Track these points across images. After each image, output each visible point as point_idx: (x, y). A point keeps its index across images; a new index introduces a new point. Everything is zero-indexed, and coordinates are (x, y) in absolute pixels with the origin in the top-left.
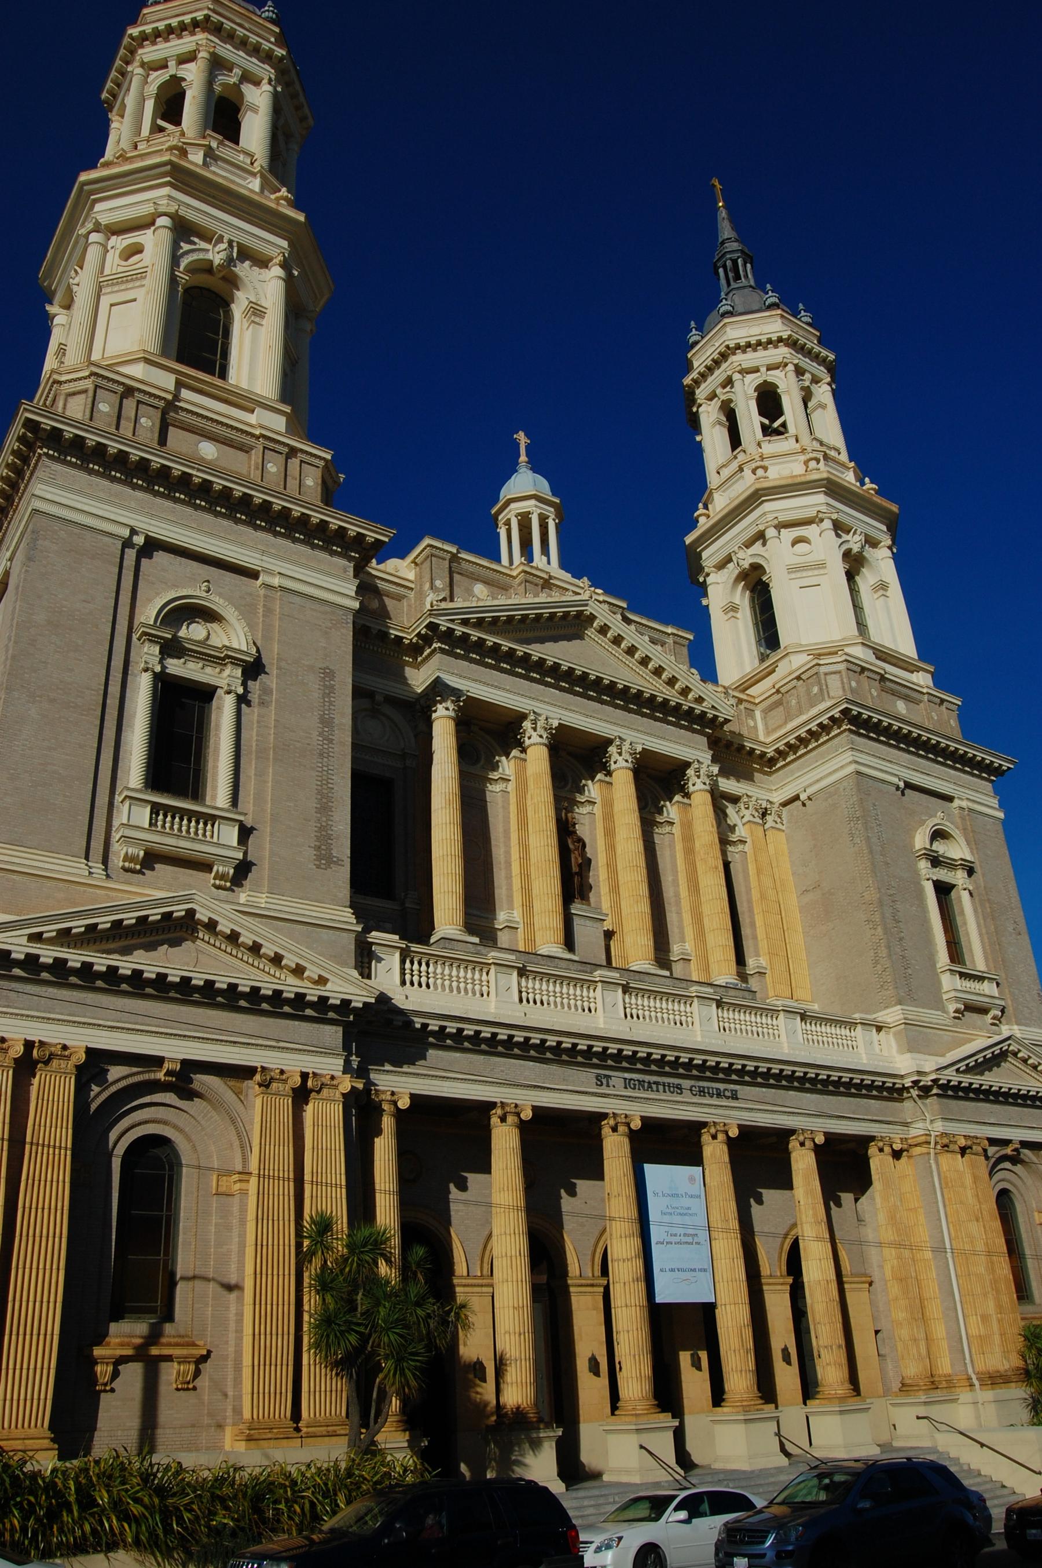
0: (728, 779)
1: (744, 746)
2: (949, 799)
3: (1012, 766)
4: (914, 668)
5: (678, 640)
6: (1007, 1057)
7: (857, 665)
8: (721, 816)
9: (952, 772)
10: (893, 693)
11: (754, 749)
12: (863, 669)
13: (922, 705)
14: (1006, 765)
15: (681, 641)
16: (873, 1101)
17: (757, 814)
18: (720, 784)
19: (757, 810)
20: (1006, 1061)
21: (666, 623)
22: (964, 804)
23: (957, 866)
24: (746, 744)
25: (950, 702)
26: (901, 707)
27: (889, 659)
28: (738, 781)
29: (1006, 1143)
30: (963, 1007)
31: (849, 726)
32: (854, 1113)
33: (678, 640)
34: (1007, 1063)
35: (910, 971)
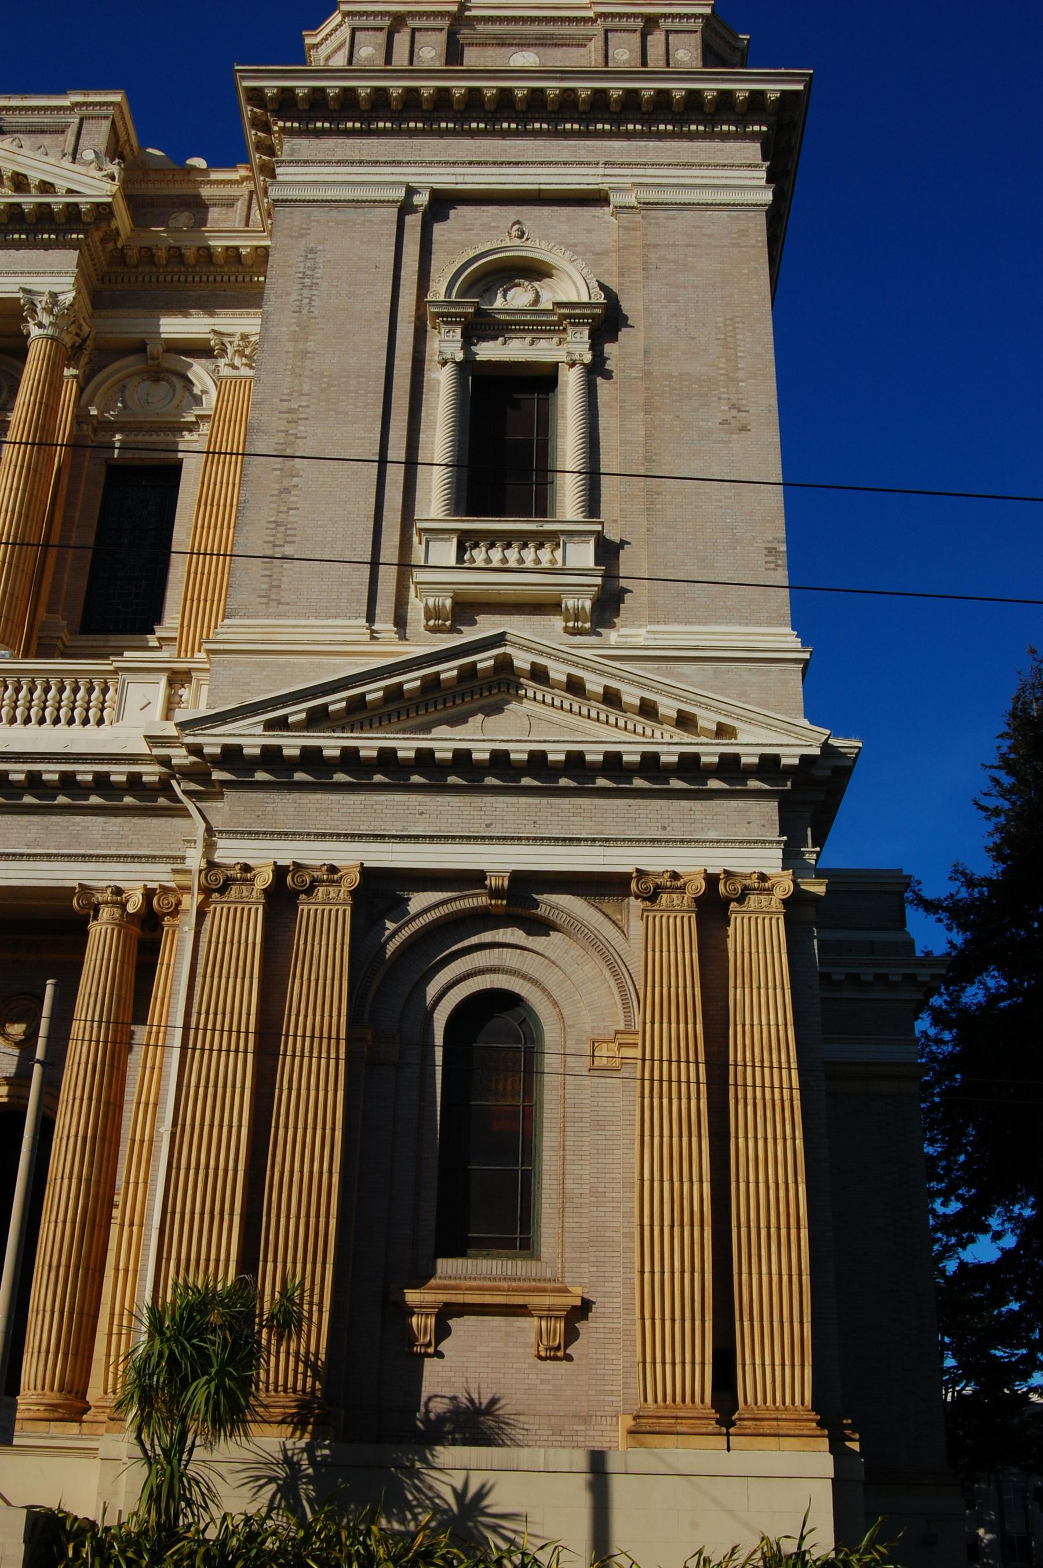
0: (186, 315)
1: (208, 248)
2: (596, 199)
3: (800, 87)
5: (91, 111)
6: (520, 686)
8: (178, 384)
9: (617, 144)
10: (501, 42)
11: (237, 248)
13: (592, 45)
14: (773, 89)
15: (97, 111)
16: (101, 819)
17: (244, 360)
19: (242, 354)
20: (520, 699)
21: (61, 90)
22: (631, 199)
24: (212, 243)
25: (673, 16)
26: (525, 59)
28: (212, 315)
29: (474, 879)
30: (448, 602)
31: (281, 124)
32: (28, 846)
33: (91, 111)
34: (528, 705)
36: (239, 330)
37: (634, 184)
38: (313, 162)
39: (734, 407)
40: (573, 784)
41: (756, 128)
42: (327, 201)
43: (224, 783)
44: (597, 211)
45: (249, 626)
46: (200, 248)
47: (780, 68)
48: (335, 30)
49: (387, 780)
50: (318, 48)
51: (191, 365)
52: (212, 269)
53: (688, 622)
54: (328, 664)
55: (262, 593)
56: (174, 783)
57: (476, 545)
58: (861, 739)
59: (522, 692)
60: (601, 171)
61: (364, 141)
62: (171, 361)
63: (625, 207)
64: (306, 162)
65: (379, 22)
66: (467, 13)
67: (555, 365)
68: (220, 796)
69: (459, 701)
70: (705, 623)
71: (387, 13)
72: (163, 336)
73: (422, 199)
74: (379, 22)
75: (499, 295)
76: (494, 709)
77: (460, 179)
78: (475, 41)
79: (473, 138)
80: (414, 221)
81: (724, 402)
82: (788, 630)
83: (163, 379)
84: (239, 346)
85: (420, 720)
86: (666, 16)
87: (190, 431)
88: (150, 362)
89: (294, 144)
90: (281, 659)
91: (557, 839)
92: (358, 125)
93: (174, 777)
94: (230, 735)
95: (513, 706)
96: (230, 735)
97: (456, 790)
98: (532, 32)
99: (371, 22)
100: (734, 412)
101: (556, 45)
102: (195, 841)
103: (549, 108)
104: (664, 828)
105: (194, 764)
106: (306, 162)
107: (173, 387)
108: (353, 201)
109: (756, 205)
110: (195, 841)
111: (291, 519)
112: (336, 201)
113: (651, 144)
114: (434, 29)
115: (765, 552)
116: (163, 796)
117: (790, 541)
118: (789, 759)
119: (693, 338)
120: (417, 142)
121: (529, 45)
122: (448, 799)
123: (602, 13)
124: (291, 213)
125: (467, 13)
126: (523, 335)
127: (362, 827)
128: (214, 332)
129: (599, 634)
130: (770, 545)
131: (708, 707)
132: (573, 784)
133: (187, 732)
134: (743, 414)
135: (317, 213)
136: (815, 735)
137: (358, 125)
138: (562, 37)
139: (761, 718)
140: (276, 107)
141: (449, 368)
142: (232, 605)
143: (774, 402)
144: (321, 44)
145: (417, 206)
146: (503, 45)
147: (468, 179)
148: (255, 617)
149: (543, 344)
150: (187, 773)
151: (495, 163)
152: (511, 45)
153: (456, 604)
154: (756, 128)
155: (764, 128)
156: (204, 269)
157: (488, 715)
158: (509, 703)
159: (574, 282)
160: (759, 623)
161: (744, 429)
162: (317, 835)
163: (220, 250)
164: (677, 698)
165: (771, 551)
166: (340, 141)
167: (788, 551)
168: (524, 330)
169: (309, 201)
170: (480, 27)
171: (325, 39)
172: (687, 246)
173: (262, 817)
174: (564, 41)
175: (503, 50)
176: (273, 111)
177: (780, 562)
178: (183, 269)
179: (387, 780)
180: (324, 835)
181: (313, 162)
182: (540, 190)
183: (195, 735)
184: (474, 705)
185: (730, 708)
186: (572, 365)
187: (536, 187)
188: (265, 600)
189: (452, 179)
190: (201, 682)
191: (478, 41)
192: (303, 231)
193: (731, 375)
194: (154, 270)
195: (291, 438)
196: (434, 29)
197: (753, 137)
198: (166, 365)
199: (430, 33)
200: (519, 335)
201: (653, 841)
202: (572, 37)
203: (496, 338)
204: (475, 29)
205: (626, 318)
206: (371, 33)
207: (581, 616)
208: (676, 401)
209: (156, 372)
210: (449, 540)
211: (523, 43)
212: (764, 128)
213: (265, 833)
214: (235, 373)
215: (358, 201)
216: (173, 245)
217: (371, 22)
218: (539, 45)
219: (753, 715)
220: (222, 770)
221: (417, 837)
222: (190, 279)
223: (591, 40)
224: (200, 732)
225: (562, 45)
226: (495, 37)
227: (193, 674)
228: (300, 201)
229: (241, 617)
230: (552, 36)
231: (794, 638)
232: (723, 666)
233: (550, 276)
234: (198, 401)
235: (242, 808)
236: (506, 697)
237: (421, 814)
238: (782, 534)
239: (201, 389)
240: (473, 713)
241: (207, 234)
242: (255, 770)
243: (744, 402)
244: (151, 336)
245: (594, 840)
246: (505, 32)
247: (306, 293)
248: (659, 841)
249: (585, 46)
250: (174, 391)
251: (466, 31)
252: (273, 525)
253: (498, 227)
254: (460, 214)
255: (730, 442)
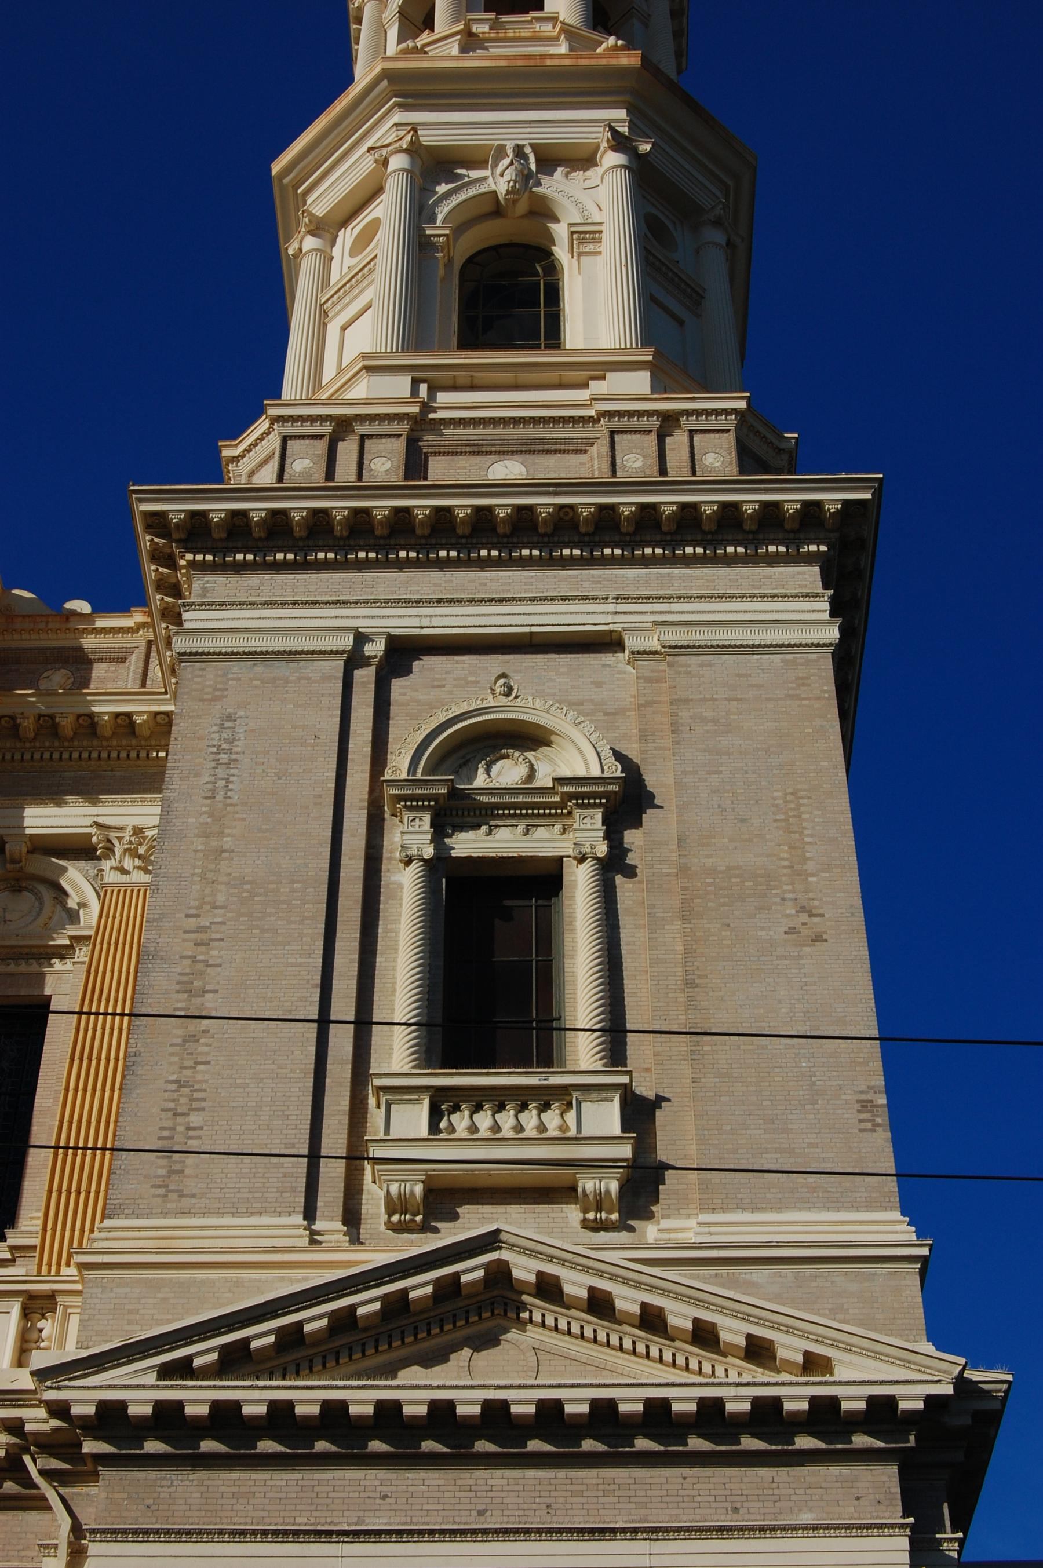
0: (59, 804)
1: (91, 716)
3: (868, 496)
4: (583, 375)
6: (522, 1306)
7: (313, 419)
8: (47, 895)
10: (477, 449)
11: (129, 715)
12: (343, 426)
13: (594, 450)
14: (832, 499)
17: (137, 862)
18: (27, 822)
19: (133, 853)
20: (522, 1325)
22: (652, 642)
23: (562, 805)
24: (96, 709)
25: (698, 413)
27: (480, 377)
28: (94, 803)
30: (419, 1189)
31: (189, 556)
34: (533, 1333)
35: (195, 1119)
36: (131, 822)
37: (655, 623)
38: (232, 604)
39: (803, 909)
40: (601, 1447)
41: (813, 548)
42: (250, 653)
43: (100, 1459)
44: (608, 658)
45: (139, 1229)
46: (79, 716)
47: (839, 472)
48: (261, 439)
49: (334, 1449)
50: (239, 461)
51: (65, 870)
52: (95, 743)
53: (754, 1209)
54: (251, 1280)
55: (159, 1181)
56: (27, 1459)
57: (456, 1108)
58: (1010, 1370)
59: (525, 1315)
60: (611, 607)
61: (298, 576)
62: (38, 865)
63: (645, 653)
64: (222, 604)
65: (317, 429)
66: (432, 416)
67: (559, 860)
68: (92, 1477)
69: (435, 1331)
70: (779, 1209)
71: (329, 418)
72: (28, 831)
73: (376, 649)
74: (317, 429)
75: (481, 771)
76: (487, 1341)
77: (425, 622)
78: (442, 449)
79: (441, 569)
80: (365, 677)
81: (790, 903)
82: (897, 1215)
83: (27, 889)
84: (131, 843)
85: (381, 1359)
86: (688, 413)
87: (62, 958)
88: (8, 866)
89: (207, 582)
90: (184, 1275)
91: (581, 1531)
92: (290, 556)
93: (27, 1451)
94: (110, 1387)
95: (513, 1335)
96: (110, 1387)
97: (433, 1460)
98: (516, 437)
99: (308, 429)
100: (804, 917)
101: (548, 452)
102: (56, 1546)
103: (541, 530)
104: (736, 1510)
105: (56, 1430)
106: (222, 604)
107: (39, 898)
108: (285, 652)
109: (818, 645)
110: (56, 1546)
111: (199, 1077)
112: (261, 653)
113: (676, 571)
114: (390, 436)
115: (858, 1106)
116: (11, 1479)
117: (890, 1089)
118: (911, 1403)
119: (743, 821)
120: (369, 576)
121: (513, 453)
122: (422, 1474)
123: (606, 411)
124: (203, 669)
125: (432, 416)
126: (514, 822)
127: (298, 1520)
128: (97, 824)
129: (631, 1229)
130: (863, 1097)
131: (789, 1330)
132: (601, 1447)
133: (48, 1384)
134: (816, 919)
135: (236, 669)
136: (944, 1366)
137: (290, 556)
138: (556, 442)
139: (866, 1343)
140: (183, 536)
141: (415, 867)
142: (115, 1200)
143: (858, 902)
144: (242, 456)
145: (369, 657)
146: (479, 453)
147: (436, 622)
148: (148, 1216)
149: (541, 833)
150: (46, 1445)
151: (471, 601)
152: (490, 453)
153: (429, 1191)
154: (813, 548)
155: (823, 548)
156: (85, 743)
157: (477, 1349)
158: (506, 1331)
159: (581, 752)
160: (855, 1207)
161: (818, 939)
162: (233, 1533)
163: (106, 718)
164: (746, 1318)
165: (866, 1105)
166: (267, 577)
167: (889, 1105)
168: (515, 816)
169: (226, 654)
170: (449, 432)
171: (248, 450)
172: (729, 700)
173: (154, 1508)
174: (558, 447)
175: (479, 459)
176: (178, 541)
177: (879, 1120)
178: (56, 744)
179: (334, 1449)
180: (243, 1533)
181: (232, 604)
182: (531, 633)
183: (59, 1388)
184: (460, 1334)
185: (821, 1330)
186: (582, 859)
187: (527, 629)
188: (161, 1191)
189: (415, 622)
190: (69, 1311)
191: (446, 449)
192: (217, 693)
193: (798, 867)
194: (18, 745)
195: (200, 966)
196: (390, 436)
197: (809, 559)
198: (31, 869)
199: (384, 440)
200: (509, 822)
201: (721, 1529)
202: (568, 441)
203: (477, 827)
204: (442, 435)
205: (651, 796)
206: (307, 442)
207: (605, 1205)
208: (723, 905)
209: (17, 880)
210: (418, 1101)
211: (505, 450)
212: (823, 548)
213: (157, 1532)
214: (124, 879)
215: (290, 653)
216: (42, 713)
217: (308, 429)
218: (526, 451)
219: (855, 1340)
220: (97, 1438)
221: (378, 1533)
222: (66, 755)
223: (592, 444)
224: (67, 1383)
225: (556, 452)
226: (469, 443)
227: (59, 1299)
228: (214, 654)
229: (127, 1216)
230: (542, 441)
231: (905, 1227)
232: (808, 1270)
233: (548, 744)
234: (73, 917)
235: (125, 1495)
236: (504, 1323)
237: (385, 1497)
238: (879, 1081)
239: (77, 900)
240: (456, 1347)
241: (89, 698)
242: (145, 1438)
243: (816, 903)
244: (12, 831)
245: (635, 1531)
246: (481, 437)
247: (221, 772)
248: (730, 1529)
249: (586, 452)
250: (41, 904)
251: (430, 438)
252: (174, 1086)
253: (478, 682)
254: (425, 666)
255: (800, 957)
